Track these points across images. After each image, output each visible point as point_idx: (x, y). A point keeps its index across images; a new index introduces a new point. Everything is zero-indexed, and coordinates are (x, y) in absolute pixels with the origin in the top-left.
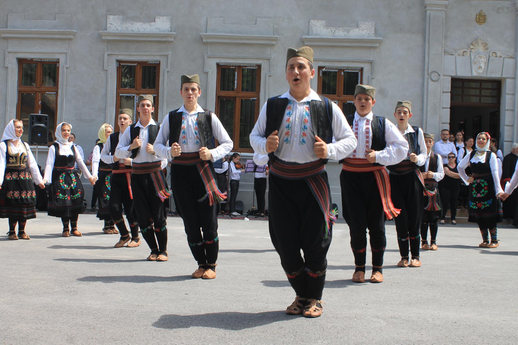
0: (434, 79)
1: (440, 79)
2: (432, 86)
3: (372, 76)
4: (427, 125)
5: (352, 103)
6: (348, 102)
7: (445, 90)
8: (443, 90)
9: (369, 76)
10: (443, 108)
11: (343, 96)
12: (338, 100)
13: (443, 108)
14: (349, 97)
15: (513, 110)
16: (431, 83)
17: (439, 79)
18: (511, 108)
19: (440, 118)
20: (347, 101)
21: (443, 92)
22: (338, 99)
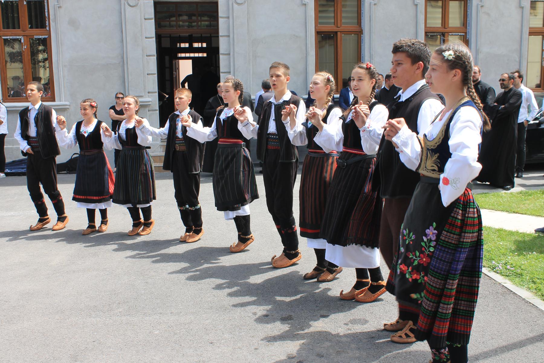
0: (131, 4)
1: (139, 4)
2: (129, 12)
3: (58, 4)
4: (128, 59)
5: (41, 38)
6: (36, 37)
7: (146, 17)
8: (144, 16)
9: (54, 5)
10: (146, 38)
11: (29, 31)
12: (23, 36)
13: (146, 38)
14: (36, 31)
15: (229, 36)
16: (128, 9)
17: (138, 3)
18: (226, 34)
19: (143, 51)
20: (33, 36)
21: (145, 19)
22: (23, 35)
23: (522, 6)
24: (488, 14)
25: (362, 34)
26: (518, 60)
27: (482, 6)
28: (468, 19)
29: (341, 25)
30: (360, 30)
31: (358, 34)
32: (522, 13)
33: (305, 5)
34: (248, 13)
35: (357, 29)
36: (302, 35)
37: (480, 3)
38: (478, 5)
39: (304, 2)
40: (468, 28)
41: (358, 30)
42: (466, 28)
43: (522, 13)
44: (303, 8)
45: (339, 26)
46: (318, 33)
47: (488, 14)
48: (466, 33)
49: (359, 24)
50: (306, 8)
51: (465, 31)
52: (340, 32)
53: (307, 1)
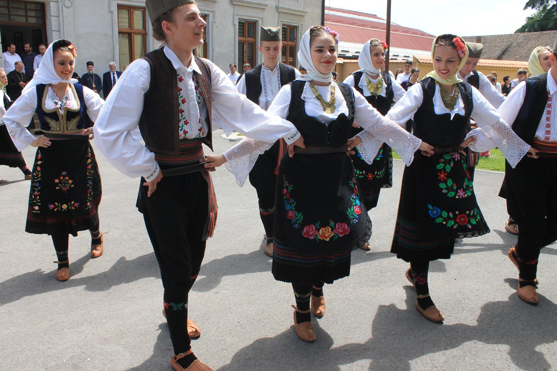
18: (57, 29)
23: (235, 24)
24: (218, 27)
25: (147, 35)
26: (233, 57)
27: (215, 22)
28: (206, 30)
29: (133, 28)
30: (145, 33)
31: (144, 35)
32: (235, 28)
33: (112, 12)
34: (73, 15)
35: (144, 32)
36: (110, 33)
37: (214, 20)
38: (212, 21)
39: (111, 10)
40: (206, 35)
41: (144, 33)
42: (205, 35)
43: (235, 28)
44: (110, 14)
45: (132, 29)
46: (119, 33)
47: (218, 27)
48: (205, 38)
49: (144, 28)
50: (112, 14)
51: (205, 37)
52: (133, 33)
53: (113, 10)
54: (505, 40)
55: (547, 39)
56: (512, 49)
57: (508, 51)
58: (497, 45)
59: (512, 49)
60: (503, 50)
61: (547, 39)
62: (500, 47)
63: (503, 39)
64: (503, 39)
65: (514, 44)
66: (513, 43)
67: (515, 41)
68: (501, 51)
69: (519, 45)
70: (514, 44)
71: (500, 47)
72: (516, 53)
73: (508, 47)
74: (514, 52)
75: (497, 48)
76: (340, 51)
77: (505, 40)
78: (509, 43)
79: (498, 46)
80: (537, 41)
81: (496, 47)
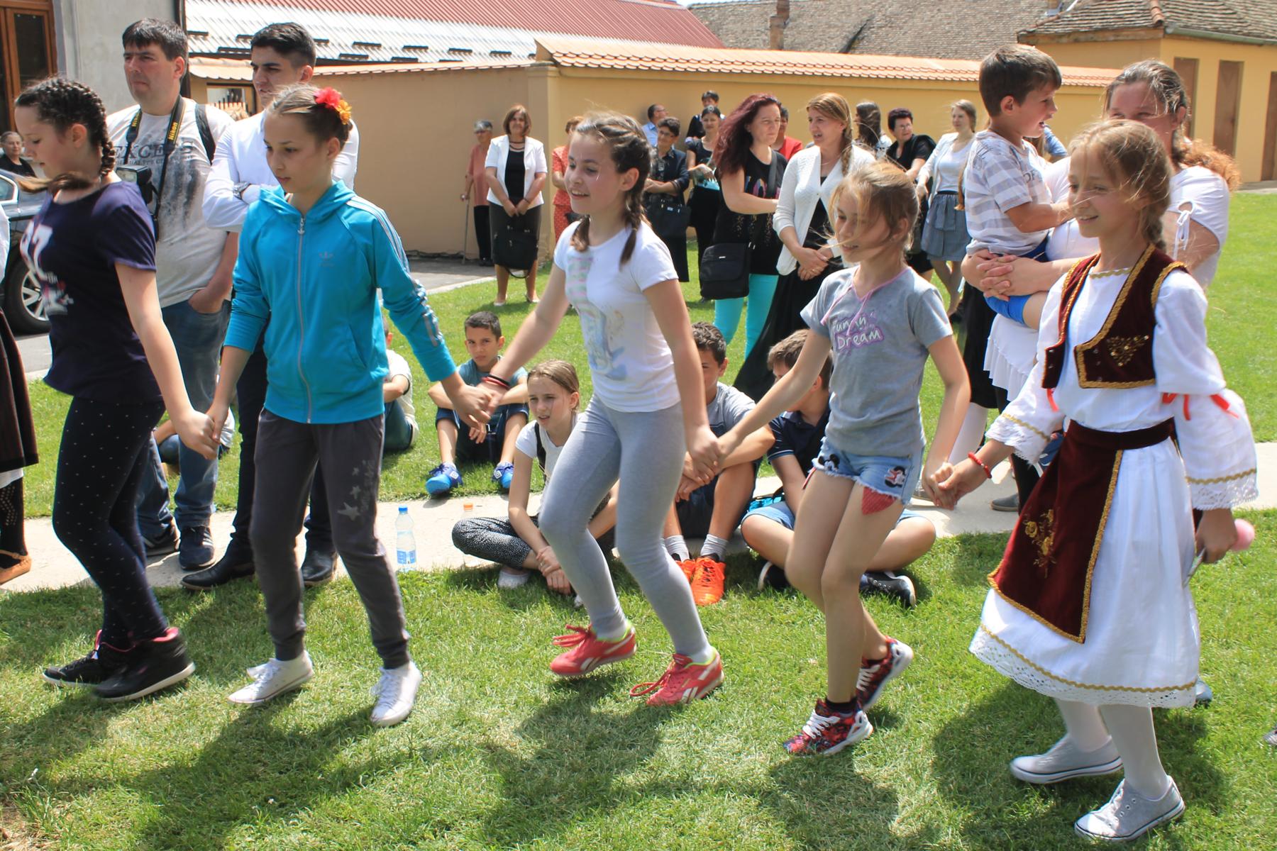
54: (854, 9)
55: (960, 6)
56: (872, 33)
57: (863, 38)
58: (834, 21)
59: (872, 33)
60: (851, 37)
61: (960, 6)
62: (843, 26)
63: (849, 6)
64: (849, 6)
65: (878, 20)
66: (873, 17)
67: (879, 11)
68: (843, 38)
69: (890, 22)
70: (877, 18)
71: (843, 26)
72: (884, 45)
73: (862, 29)
74: (879, 41)
75: (833, 32)
76: (400, 49)
77: (854, 9)
78: (865, 17)
79: (835, 26)
80: (935, 11)
81: (830, 27)
